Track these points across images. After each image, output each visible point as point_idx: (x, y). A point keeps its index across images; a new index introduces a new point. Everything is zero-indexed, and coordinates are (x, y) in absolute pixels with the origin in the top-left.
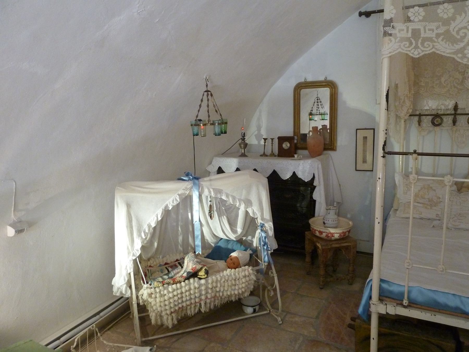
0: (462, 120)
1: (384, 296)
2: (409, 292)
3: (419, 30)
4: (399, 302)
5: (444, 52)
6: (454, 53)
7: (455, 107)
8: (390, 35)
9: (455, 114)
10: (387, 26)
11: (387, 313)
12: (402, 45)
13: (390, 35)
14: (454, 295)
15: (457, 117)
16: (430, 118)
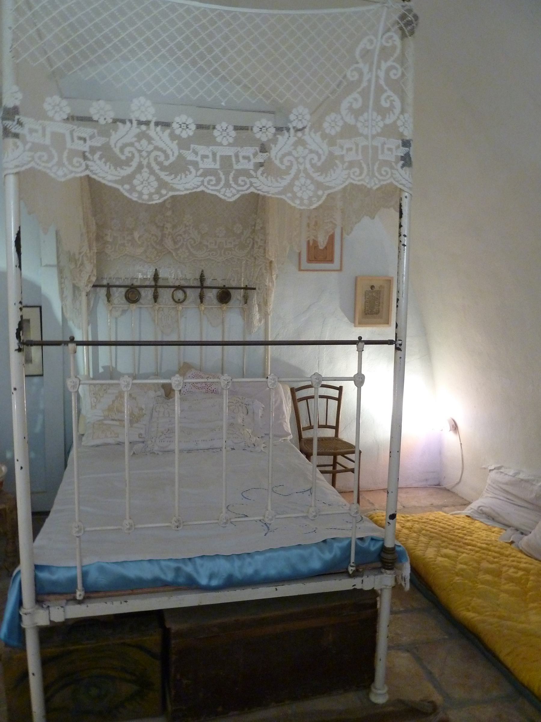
0: (165, 295)
1: (43, 594)
2: (85, 575)
3: (63, 135)
4: (69, 597)
5: (103, 178)
7: (155, 276)
8: (16, 136)
9: (156, 287)
10: (8, 119)
11: (51, 621)
13: (16, 136)
14: (150, 561)
15: (160, 290)
16: (123, 290)
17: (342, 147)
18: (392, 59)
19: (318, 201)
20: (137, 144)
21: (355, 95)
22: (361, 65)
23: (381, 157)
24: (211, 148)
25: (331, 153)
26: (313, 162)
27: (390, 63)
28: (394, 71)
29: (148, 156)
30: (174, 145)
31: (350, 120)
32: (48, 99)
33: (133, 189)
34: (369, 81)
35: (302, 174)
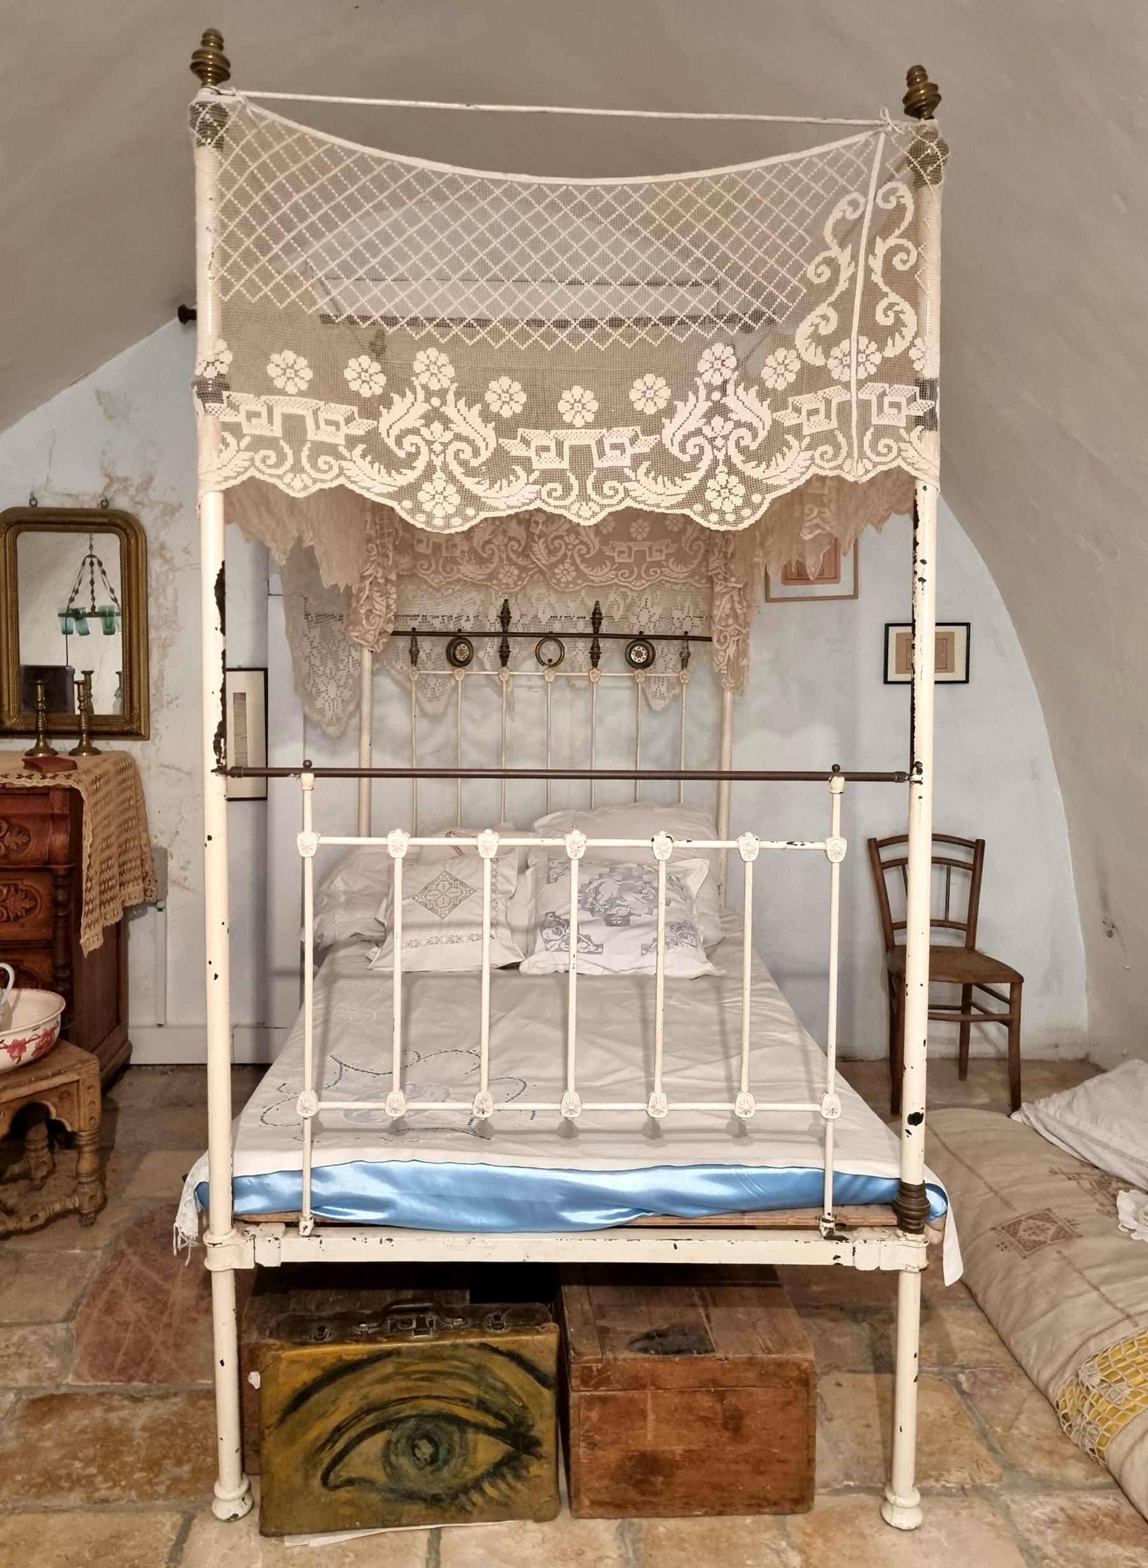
3: (301, 419)
5: (368, 489)
6: (390, 496)
12: (258, 457)
17: (797, 410)
18: (897, 232)
19: (753, 514)
20: (424, 431)
21: (823, 308)
22: (834, 251)
23: (875, 420)
24: (553, 432)
25: (776, 424)
26: (742, 443)
27: (892, 241)
28: (902, 255)
29: (443, 451)
30: (489, 431)
31: (815, 358)
32: (275, 358)
33: (417, 508)
34: (853, 279)
35: (722, 468)
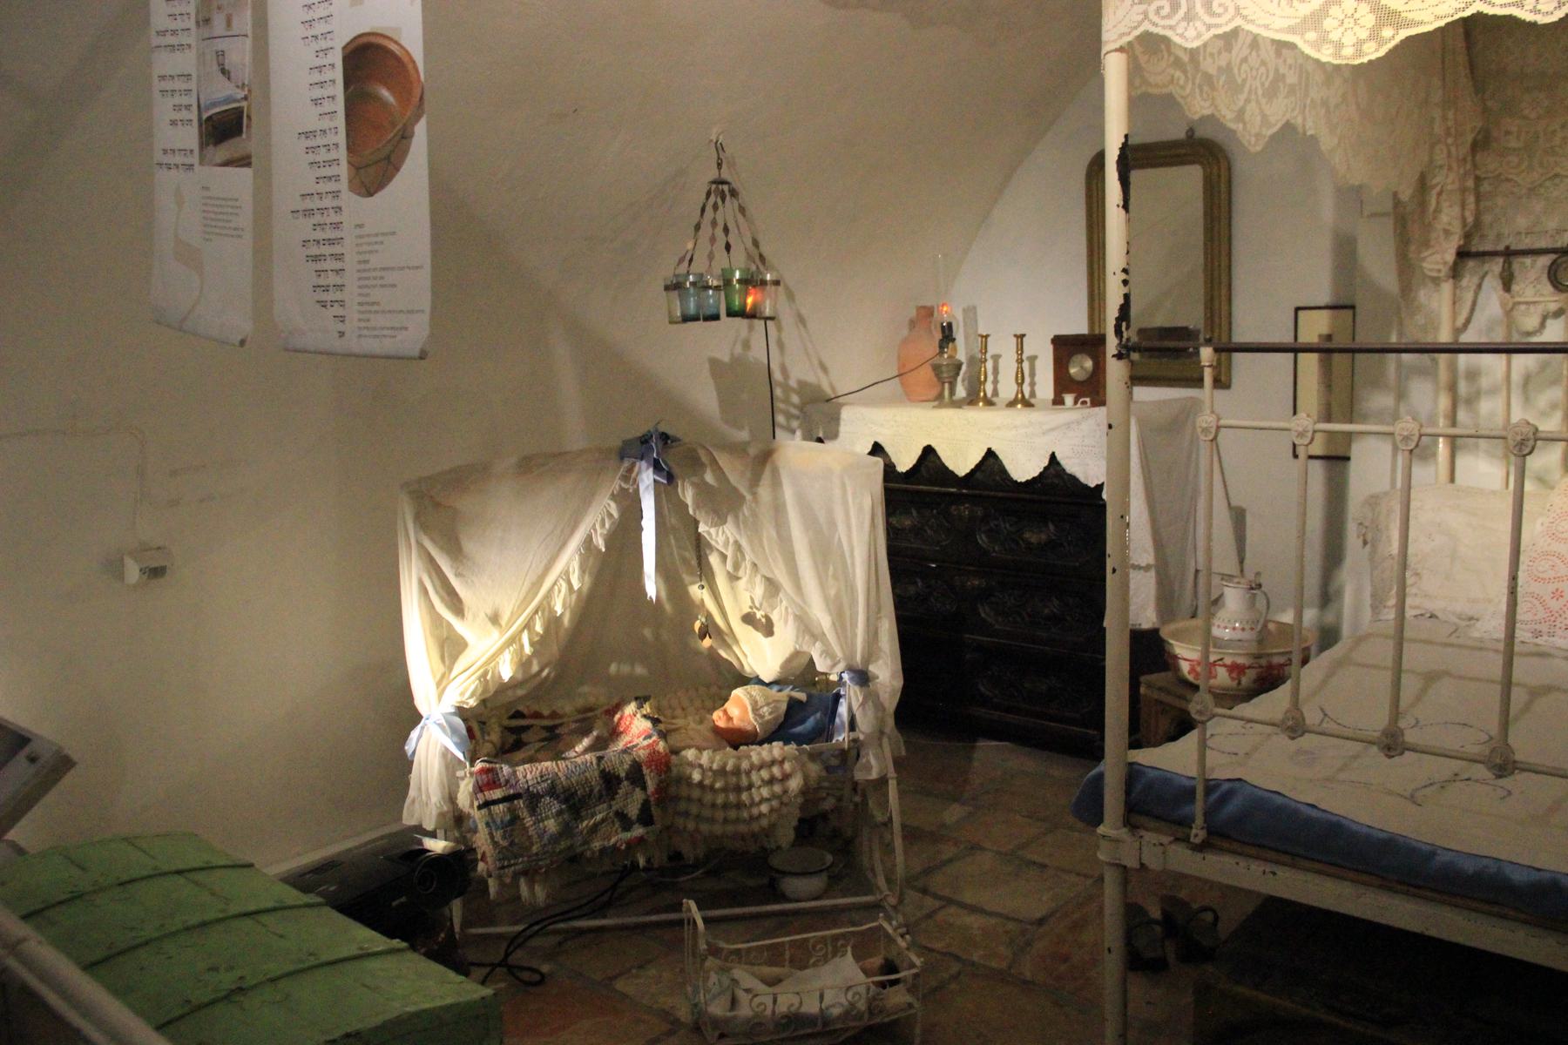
5: (1267, 27)
6: (1291, 30)
16: (1545, 261)
33: (1323, 39)
